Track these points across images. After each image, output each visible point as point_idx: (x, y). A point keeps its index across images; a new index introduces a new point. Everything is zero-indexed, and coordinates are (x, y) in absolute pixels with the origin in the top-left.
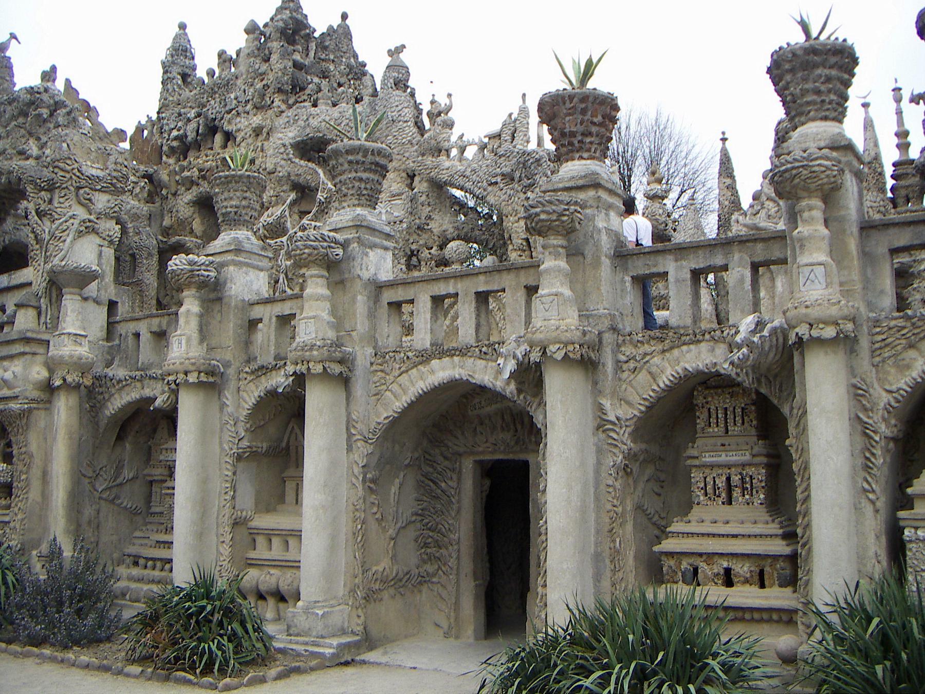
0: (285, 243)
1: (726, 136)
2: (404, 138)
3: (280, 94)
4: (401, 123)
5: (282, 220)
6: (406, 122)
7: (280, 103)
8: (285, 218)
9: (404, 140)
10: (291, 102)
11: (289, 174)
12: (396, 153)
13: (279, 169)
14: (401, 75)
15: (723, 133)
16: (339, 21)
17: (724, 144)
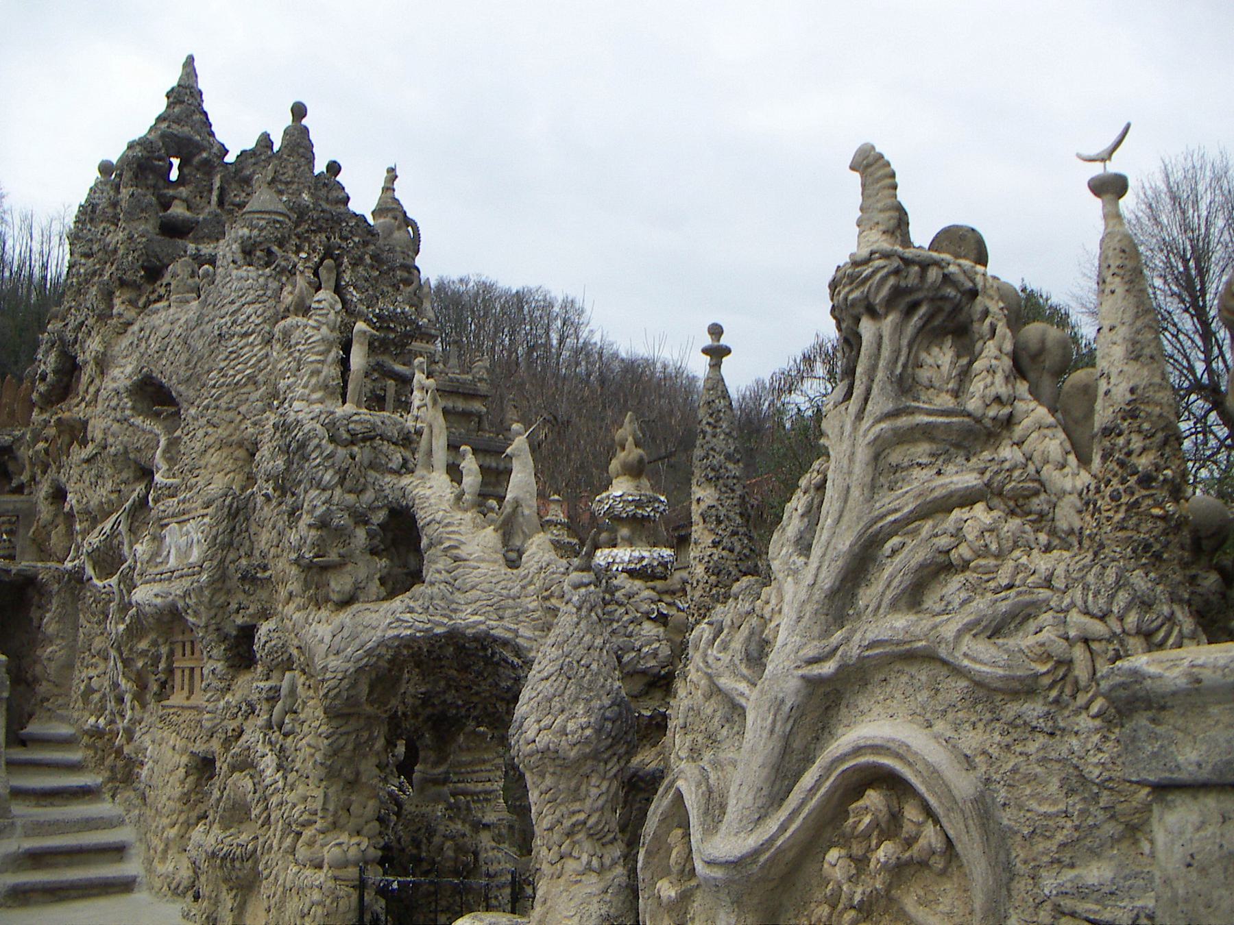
0: (115, 589)
1: (724, 341)
2: (239, 372)
3: (125, 290)
4: (235, 339)
5: (115, 542)
6: (246, 335)
7: (123, 307)
8: (119, 538)
9: (238, 377)
10: (140, 304)
11: (126, 448)
12: (224, 406)
13: (111, 440)
14: (256, 232)
15: (716, 331)
16: (288, 120)
17: (716, 366)
